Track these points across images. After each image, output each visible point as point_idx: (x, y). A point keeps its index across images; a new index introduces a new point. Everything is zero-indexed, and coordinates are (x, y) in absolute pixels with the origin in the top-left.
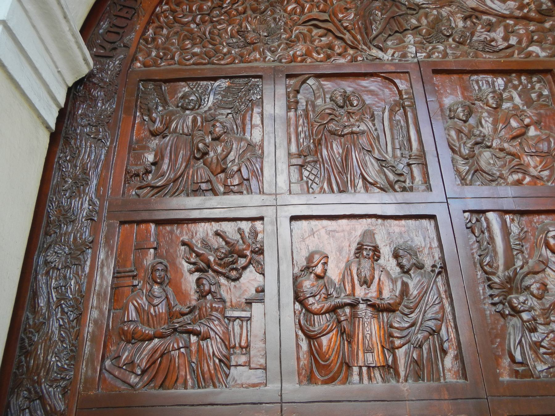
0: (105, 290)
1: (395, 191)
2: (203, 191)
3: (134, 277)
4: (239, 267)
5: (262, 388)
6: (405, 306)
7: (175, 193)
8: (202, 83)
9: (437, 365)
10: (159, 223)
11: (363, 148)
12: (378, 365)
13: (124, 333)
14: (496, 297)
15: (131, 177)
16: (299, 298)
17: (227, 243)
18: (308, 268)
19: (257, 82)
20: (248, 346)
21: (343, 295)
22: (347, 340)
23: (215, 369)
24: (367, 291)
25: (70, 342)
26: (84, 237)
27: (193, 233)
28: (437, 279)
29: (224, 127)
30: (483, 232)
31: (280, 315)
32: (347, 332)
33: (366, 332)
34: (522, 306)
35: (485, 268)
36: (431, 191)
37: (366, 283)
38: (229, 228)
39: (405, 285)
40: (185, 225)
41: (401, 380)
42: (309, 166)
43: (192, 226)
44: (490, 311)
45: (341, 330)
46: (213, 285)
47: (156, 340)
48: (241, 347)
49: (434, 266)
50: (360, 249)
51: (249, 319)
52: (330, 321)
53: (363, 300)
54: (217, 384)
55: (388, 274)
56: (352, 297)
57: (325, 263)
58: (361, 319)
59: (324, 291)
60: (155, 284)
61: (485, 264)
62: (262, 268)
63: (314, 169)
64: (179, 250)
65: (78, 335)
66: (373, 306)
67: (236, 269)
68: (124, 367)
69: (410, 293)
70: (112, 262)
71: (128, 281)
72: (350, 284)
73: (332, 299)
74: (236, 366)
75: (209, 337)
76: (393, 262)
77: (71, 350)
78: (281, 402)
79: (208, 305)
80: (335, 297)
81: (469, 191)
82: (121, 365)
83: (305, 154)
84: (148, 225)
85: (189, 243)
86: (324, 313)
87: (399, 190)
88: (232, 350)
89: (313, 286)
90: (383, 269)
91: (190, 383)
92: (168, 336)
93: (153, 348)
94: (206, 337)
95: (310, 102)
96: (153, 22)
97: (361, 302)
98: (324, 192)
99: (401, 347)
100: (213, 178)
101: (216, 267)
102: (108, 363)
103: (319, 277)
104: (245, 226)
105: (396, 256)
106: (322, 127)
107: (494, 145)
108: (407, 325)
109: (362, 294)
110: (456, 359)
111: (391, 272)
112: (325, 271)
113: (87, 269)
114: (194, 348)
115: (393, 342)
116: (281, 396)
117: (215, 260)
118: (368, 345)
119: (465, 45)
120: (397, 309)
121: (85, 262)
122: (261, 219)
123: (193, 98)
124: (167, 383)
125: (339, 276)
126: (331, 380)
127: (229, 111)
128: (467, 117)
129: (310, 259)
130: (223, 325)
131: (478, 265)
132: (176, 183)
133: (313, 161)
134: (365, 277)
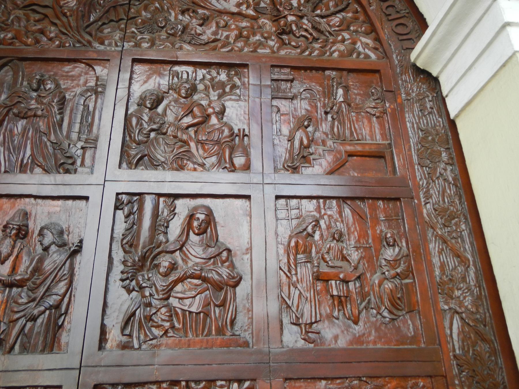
1: (59, 173)
14: (125, 273)
34: (145, 282)
36: (92, 173)
81: (126, 174)
119: (176, 37)
128: (152, 105)
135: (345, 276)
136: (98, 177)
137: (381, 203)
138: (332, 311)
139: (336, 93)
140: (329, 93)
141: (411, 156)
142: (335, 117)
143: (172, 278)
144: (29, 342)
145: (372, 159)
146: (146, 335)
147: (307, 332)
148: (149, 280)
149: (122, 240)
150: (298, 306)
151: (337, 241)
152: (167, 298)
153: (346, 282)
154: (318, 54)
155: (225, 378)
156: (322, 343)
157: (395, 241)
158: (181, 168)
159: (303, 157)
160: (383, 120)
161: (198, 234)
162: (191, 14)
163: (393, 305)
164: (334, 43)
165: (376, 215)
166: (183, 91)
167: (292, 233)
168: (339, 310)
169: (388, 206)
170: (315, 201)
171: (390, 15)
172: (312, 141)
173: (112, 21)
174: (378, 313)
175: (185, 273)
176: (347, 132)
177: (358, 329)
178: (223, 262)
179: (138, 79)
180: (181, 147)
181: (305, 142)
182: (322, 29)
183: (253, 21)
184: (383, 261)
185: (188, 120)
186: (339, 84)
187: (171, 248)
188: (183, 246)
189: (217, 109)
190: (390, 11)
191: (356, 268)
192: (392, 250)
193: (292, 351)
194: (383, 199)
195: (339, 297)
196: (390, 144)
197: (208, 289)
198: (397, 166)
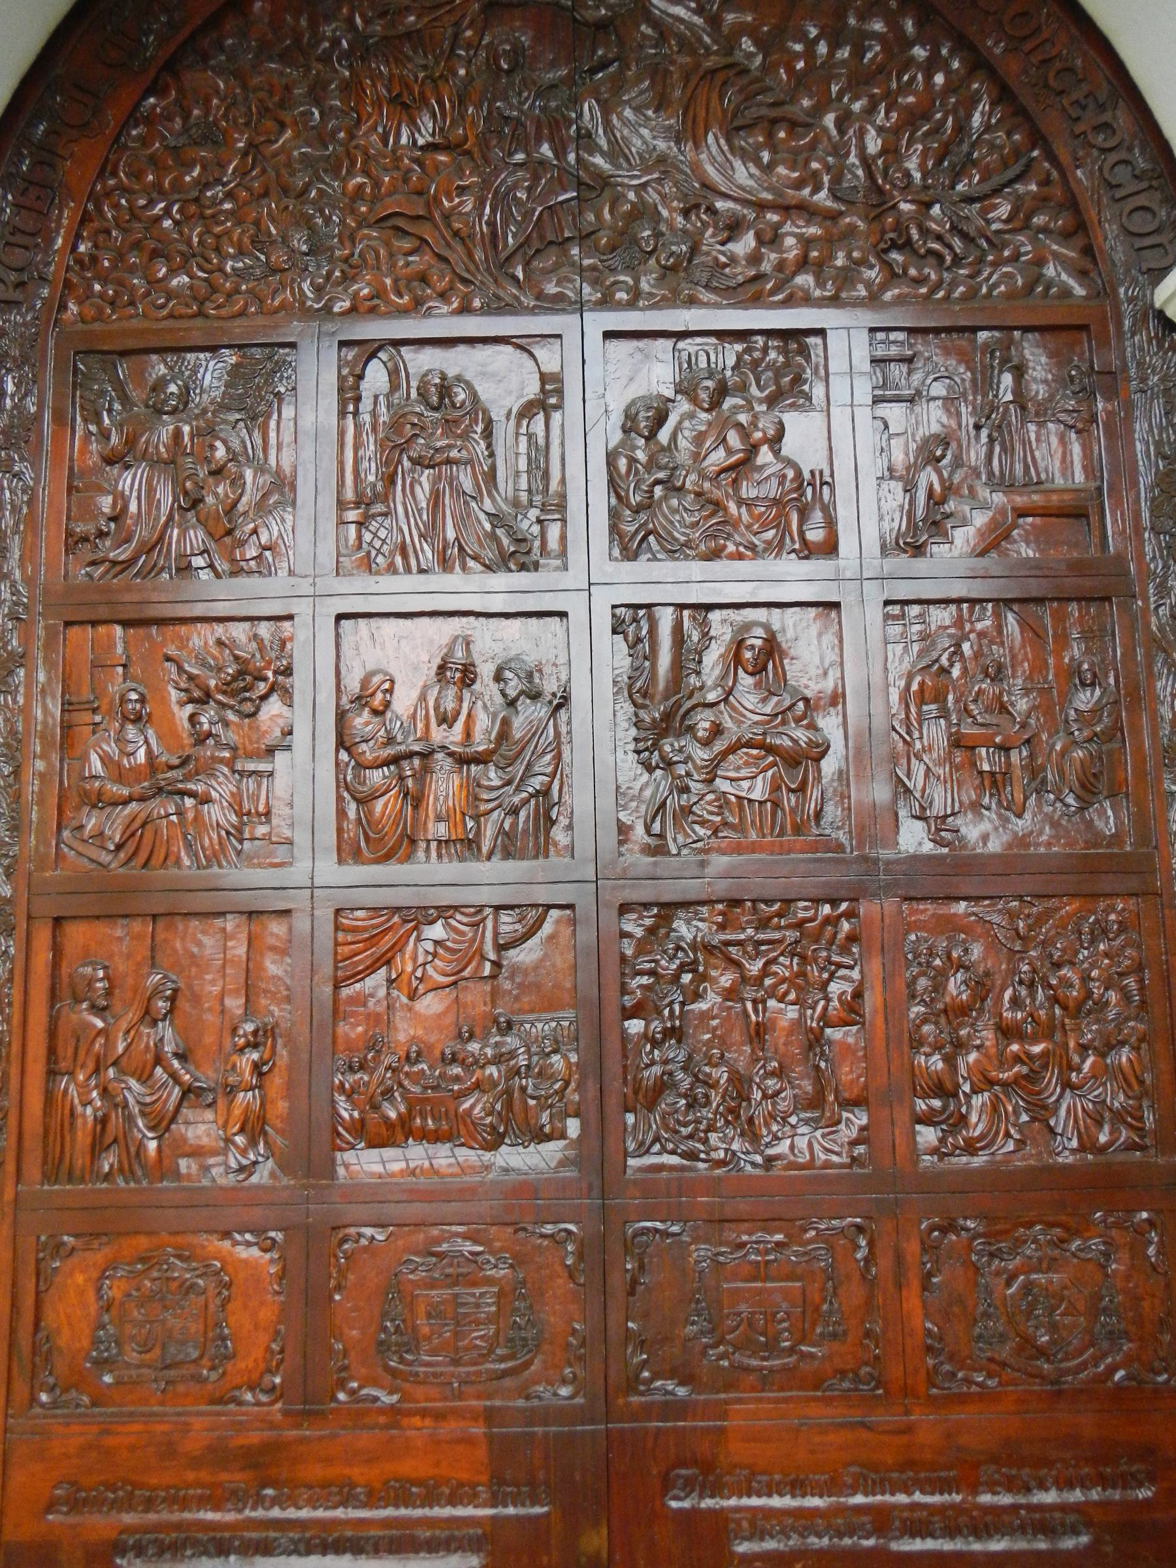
1: (511, 571)
3: (95, 711)
8: (189, 356)
9: (537, 838)
10: (126, 624)
13: (86, 794)
15: (76, 543)
16: (342, 742)
18: (359, 698)
20: (268, 814)
21: (411, 738)
23: (220, 843)
29: (228, 449)
37: (446, 720)
38: (239, 632)
39: (506, 722)
43: (183, 630)
48: (259, 814)
49: (554, 695)
50: (442, 668)
51: (271, 774)
57: (390, 691)
65: (18, 797)
66: (451, 754)
71: (86, 717)
74: (252, 839)
76: (494, 688)
77: (13, 818)
78: (312, 887)
86: (380, 766)
87: (513, 567)
91: (186, 862)
94: (206, 800)
96: (91, 221)
100: (212, 546)
101: (220, 697)
102: (66, 834)
105: (498, 677)
107: (688, 484)
108: (499, 783)
112: (387, 704)
114: (190, 815)
121: (17, 687)
122: (290, 617)
123: (173, 388)
124: (153, 862)
127: (238, 416)
128: (650, 432)
129: (365, 683)
133: (381, 514)
135: (1003, 740)
136: (575, 577)
137: (1073, 608)
138: (979, 797)
139: (999, 383)
140: (985, 383)
141: (1137, 514)
142: (995, 434)
143: (719, 746)
144: (515, 845)
145: (1064, 520)
146: (687, 835)
147: (938, 830)
148: (681, 750)
149: (630, 687)
150: (924, 790)
151: (992, 680)
152: (711, 781)
153: (1005, 749)
154: (963, 293)
155: (812, 896)
156: (964, 847)
157: (1095, 675)
158: (714, 555)
159: (934, 523)
160: (1089, 436)
161: (752, 674)
162: (704, 217)
163: (1083, 786)
164: (996, 264)
165: (1064, 629)
166: (704, 395)
167: (913, 666)
168: (991, 795)
169: (1088, 613)
170: (953, 608)
171: (1119, 186)
172: (949, 489)
173: (551, 243)
174: (1058, 799)
175: (739, 739)
176: (1019, 468)
177: (1021, 825)
178: (798, 720)
179: (617, 375)
180: (712, 515)
181: (937, 487)
182: (972, 233)
183: (829, 223)
184: (1072, 712)
185: (718, 457)
186: (1005, 361)
187: (711, 697)
188: (730, 693)
189: (771, 432)
190: (1122, 173)
191: (1024, 725)
192: (1088, 694)
193: (915, 858)
194: (1078, 600)
195: (992, 774)
196: (1099, 489)
197: (774, 764)
198: (1110, 533)
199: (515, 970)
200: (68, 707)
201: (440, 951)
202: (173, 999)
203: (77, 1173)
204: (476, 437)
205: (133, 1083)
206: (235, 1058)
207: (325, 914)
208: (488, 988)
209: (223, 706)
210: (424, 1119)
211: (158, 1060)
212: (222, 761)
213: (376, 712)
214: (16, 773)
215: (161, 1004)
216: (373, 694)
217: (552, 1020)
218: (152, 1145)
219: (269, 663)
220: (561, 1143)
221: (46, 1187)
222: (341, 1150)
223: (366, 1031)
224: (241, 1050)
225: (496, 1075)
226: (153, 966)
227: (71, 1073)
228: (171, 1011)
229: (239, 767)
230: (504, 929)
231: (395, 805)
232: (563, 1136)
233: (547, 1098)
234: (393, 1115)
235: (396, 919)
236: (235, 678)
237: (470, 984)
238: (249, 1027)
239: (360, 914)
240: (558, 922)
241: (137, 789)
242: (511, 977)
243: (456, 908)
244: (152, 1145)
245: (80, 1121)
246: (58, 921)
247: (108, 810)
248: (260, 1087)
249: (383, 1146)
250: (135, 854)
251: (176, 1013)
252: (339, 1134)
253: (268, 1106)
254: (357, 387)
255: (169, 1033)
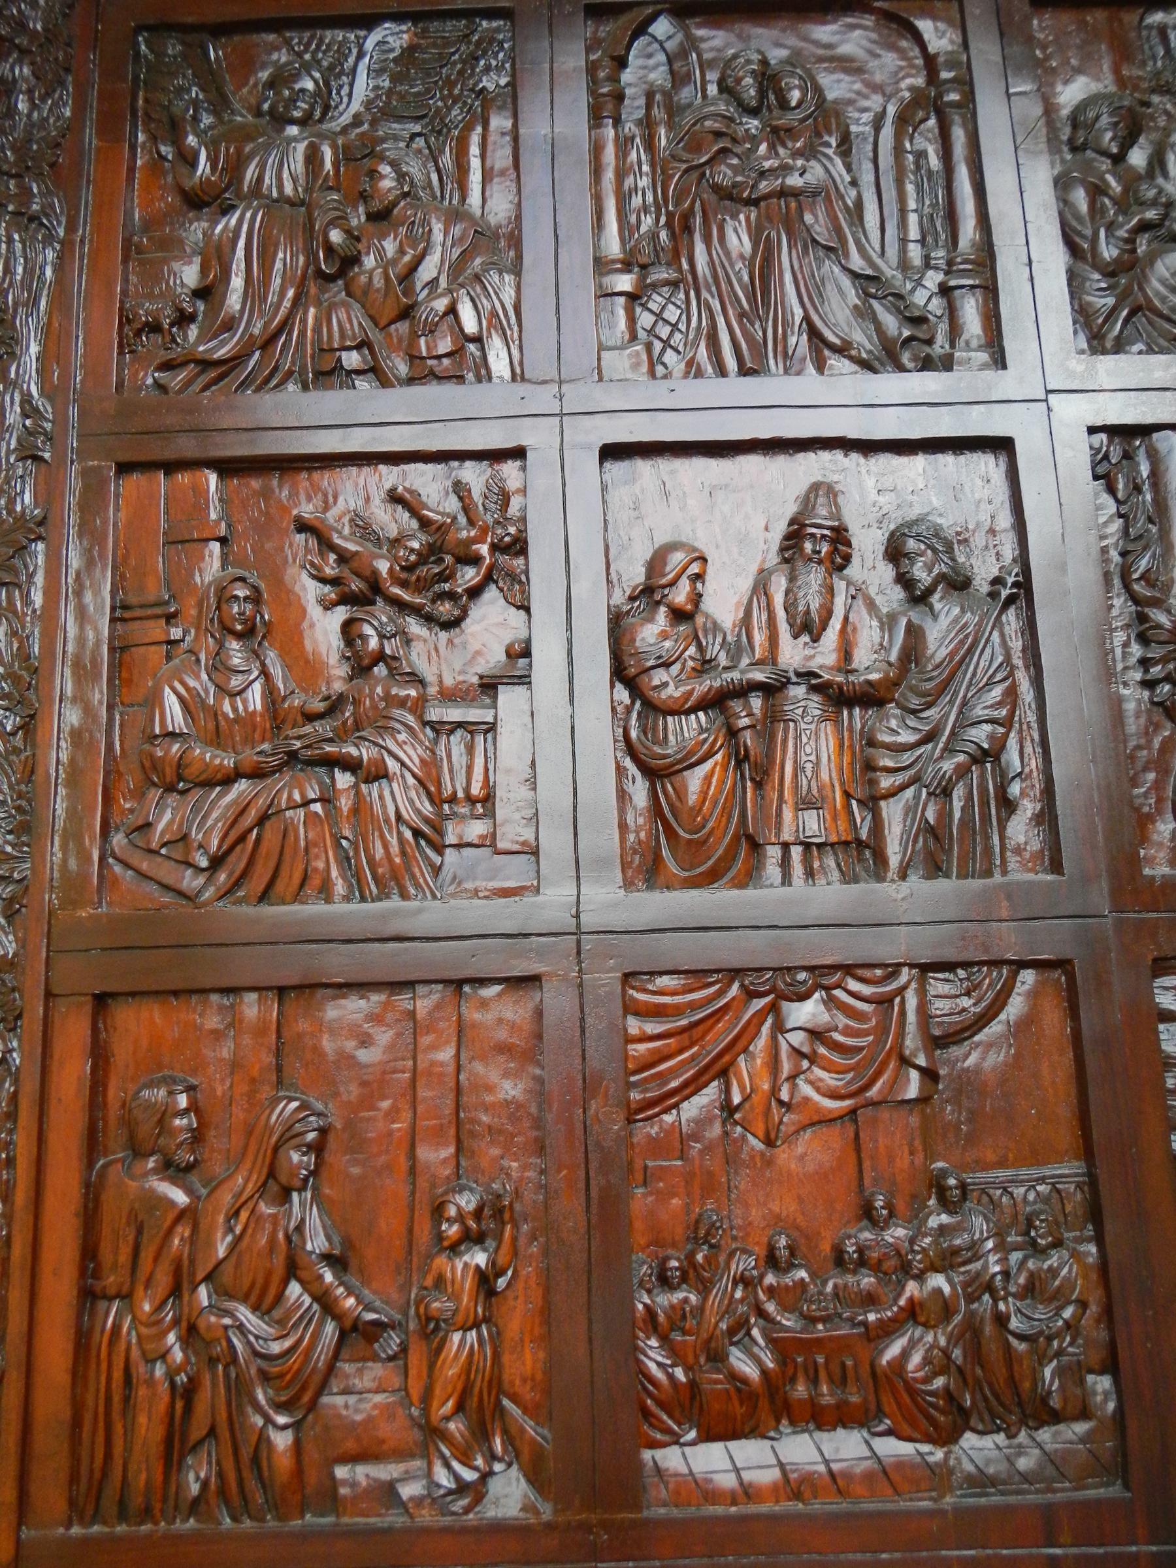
0: (93, 652)
1: (902, 369)
2: (349, 373)
3: (170, 618)
4: (460, 590)
5: (529, 899)
6: (912, 689)
7: (267, 380)
8: (329, 35)
9: (987, 838)
10: (227, 468)
11: (814, 241)
12: (833, 838)
15: (138, 333)
17: (425, 523)
19: (498, 30)
20: (488, 799)
21: (745, 661)
22: (752, 779)
23: (403, 853)
24: (812, 652)
25: (11, 787)
26: (19, 508)
27: (326, 495)
28: (1004, 618)
29: (401, 176)
30: (1138, 489)
31: (572, 717)
32: (752, 759)
33: (804, 758)
35: (1136, 587)
36: (1004, 367)
39: (914, 633)
40: (305, 475)
41: (890, 875)
42: (655, 296)
43: (325, 479)
44: (1139, 701)
45: (737, 753)
46: (389, 638)
47: (242, 785)
48: (471, 800)
49: (997, 581)
50: (795, 536)
51: (491, 728)
52: (707, 730)
53: (798, 674)
54: (412, 891)
55: (871, 605)
56: (769, 668)
57: (699, 577)
58: (791, 724)
59: (692, 650)
60: (229, 638)
61: (1135, 576)
62: (523, 592)
63: (670, 306)
64: (291, 545)
65: (30, 771)
67: (452, 596)
68: (163, 851)
69: (929, 652)
70: (104, 576)
71: (156, 630)
72: (766, 632)
73: (713, 674)
74: (459, 846)
75: (382, 773)
76: (887, 572)
77: (19, 809)
78: (578, 932)
79: (379, 690)
80: (725, 668)
82: (154, 845)
83: (644, 260)
84: (198, 473)
85: (317, 524)
86: (694, 710)
87: (909, 365)
88: (446, 807)
89: (664, 636)
90: (858, 593)
91: (340, 888)
92: (274, 772)
93: (235, 802)
94: (378, 774)
95: (658, 97)
97: (794, 679)
98: (699, 374)
99: (893, 795)
100: (375, 335)
101: (396, 590)
102: (118, 840)
103: (679, 615)
104: (473, 475)
105: (895, 553)
106: (695, 175)
109: (797, 658)
110: (1038, 824)
111: (879, 600)
112: (696, 598)
113: (38, 599)
114: (345, 803)
115: (873, 783)
116: (578, 916)
117: (391, 570)
118: (809, 790)
120: (889, 696)
121: (31, 576)
125: (737, 610)
126: (710, 878)
127: (417, 128)
129: (655, 564)
130: (421, 743)
131: (1117, 582)
132: (270, 349)
133: (667, 283)
134: (808, 612)
199: (968, 1083)
200: (121, 613)
201: (822, 1050)
202: (318, 1148)
203: (136, 1501)
204: (830, 152)
205: (244, 1313)
206: (441, 1261)
207: (605, 979)
208: (914, 1120)
209: (401, 606)
210: (815, 1381)
211: (293, 1269)
212: (402, 703)
213: (679, 615)
214: (28, 727)
215: (295, 1157)
216: (673, 583)
217: (1042, 1180)
218: (282, 1441)
219: (484, 530)
220: (1081, 1428)
221: (76, 1530)
222: (654, 1445)
223: (687, 1208)
224: (454, 1249)
225: (947, 1289)
226: (280, 1083)
227: (127, 1296)
228: (314, 1173)
229: (433, 714)
230: (940, 1007)
231: (722, 782)
232: (1084, 1414)
233: (1050, 1339)
234: (750, 1370)
235: (735, 989)
236: (423, 559)
237: (885, 1114)
238: (467, 1201)
239: (664, 981)
240: (1034, 995)
241: (250, 756)
242: (956, 1101)
243: (849, 969)
244: (282, 1441)
245: (142, 1392)
246: (101, 1001)
247: (197, 793)
248: (487, 1320)
249: (735, 1435)
250: (245, 874)
251: (324, 1174)
252: (646, 1414)
253: (506, 1359)
254: (614, 79)
255: (314, 1220)
